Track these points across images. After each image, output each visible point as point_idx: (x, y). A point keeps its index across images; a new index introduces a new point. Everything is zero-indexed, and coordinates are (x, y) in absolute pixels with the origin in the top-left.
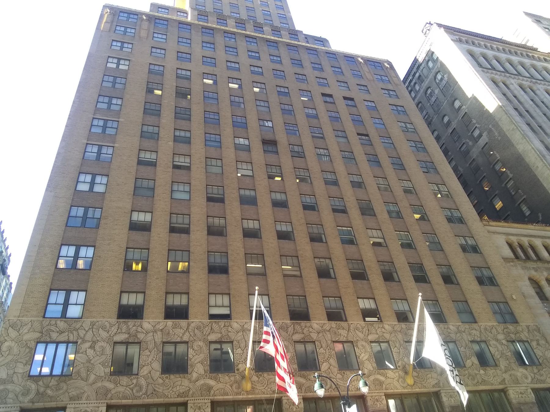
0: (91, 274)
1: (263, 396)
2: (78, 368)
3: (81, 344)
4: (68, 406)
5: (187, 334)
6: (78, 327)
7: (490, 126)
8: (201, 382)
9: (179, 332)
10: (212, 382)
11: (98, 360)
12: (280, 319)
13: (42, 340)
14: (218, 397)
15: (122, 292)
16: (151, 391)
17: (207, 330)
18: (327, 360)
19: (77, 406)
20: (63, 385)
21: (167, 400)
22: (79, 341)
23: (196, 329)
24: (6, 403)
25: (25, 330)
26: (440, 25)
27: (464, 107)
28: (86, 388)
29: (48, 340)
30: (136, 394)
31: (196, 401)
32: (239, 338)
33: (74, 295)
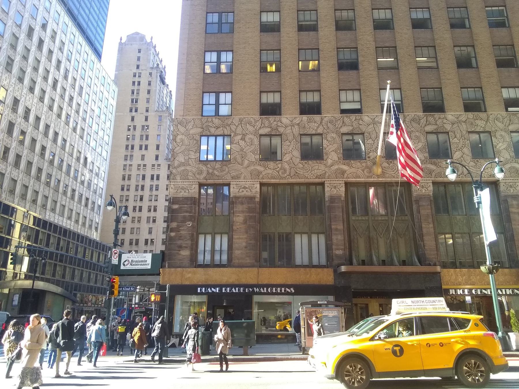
0: (234, 77)
1: (393, 179)
2: (234, 155)
3: (233, 136)
4: (231, 183)
5: (321, 127)
6: (229, 123)
9: (314, 125)
10: (345, 167)
11: (249, 149)
12: (412, 112)
13: (204, 134)
14: (351, 179)
15: (261, 92)
16: (294, 174)
17: (339, 123)
18: (461, 150)
19: (238, 183)
20: (224, 167)
21: (307, 181)
22: (232, 135)
23: (328, 123)
24: (188, 179)
25: (190, 126)
28: (242, 170)
29: (209, 134)
30: (282, 176)
31: (331, 182)
32: (370, 130)
33: (222, 96)
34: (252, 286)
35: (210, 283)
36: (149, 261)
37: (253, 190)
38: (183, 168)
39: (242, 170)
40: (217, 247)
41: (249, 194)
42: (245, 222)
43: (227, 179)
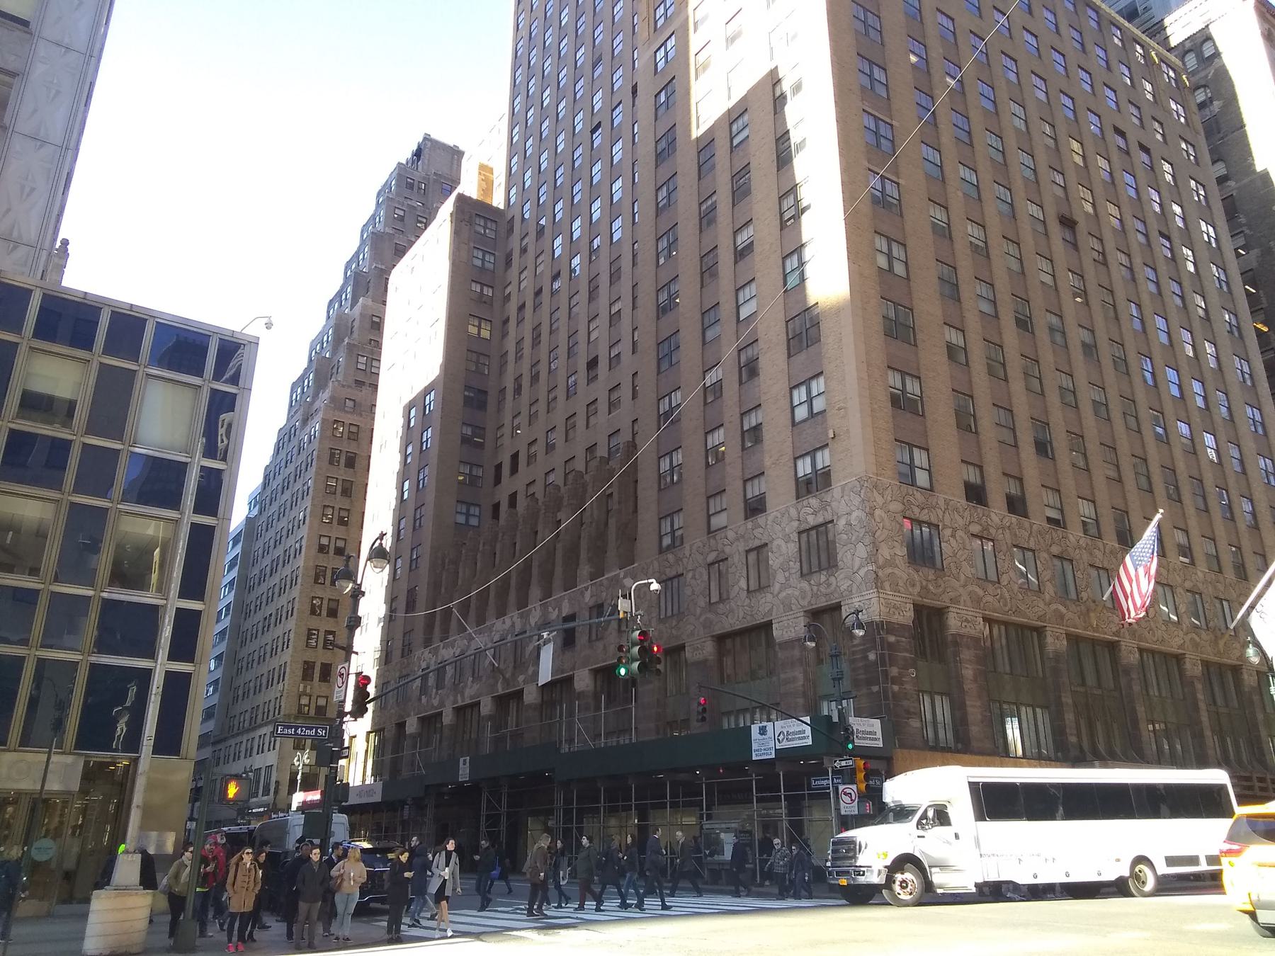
8: (1053, 607)
20: (940, 581)
36: (879, 735)
38: (889, 570)
39: (961, 590)
40: (939, 717)
41: (973, 632)
42: (975, 680)
43: (943, 601)
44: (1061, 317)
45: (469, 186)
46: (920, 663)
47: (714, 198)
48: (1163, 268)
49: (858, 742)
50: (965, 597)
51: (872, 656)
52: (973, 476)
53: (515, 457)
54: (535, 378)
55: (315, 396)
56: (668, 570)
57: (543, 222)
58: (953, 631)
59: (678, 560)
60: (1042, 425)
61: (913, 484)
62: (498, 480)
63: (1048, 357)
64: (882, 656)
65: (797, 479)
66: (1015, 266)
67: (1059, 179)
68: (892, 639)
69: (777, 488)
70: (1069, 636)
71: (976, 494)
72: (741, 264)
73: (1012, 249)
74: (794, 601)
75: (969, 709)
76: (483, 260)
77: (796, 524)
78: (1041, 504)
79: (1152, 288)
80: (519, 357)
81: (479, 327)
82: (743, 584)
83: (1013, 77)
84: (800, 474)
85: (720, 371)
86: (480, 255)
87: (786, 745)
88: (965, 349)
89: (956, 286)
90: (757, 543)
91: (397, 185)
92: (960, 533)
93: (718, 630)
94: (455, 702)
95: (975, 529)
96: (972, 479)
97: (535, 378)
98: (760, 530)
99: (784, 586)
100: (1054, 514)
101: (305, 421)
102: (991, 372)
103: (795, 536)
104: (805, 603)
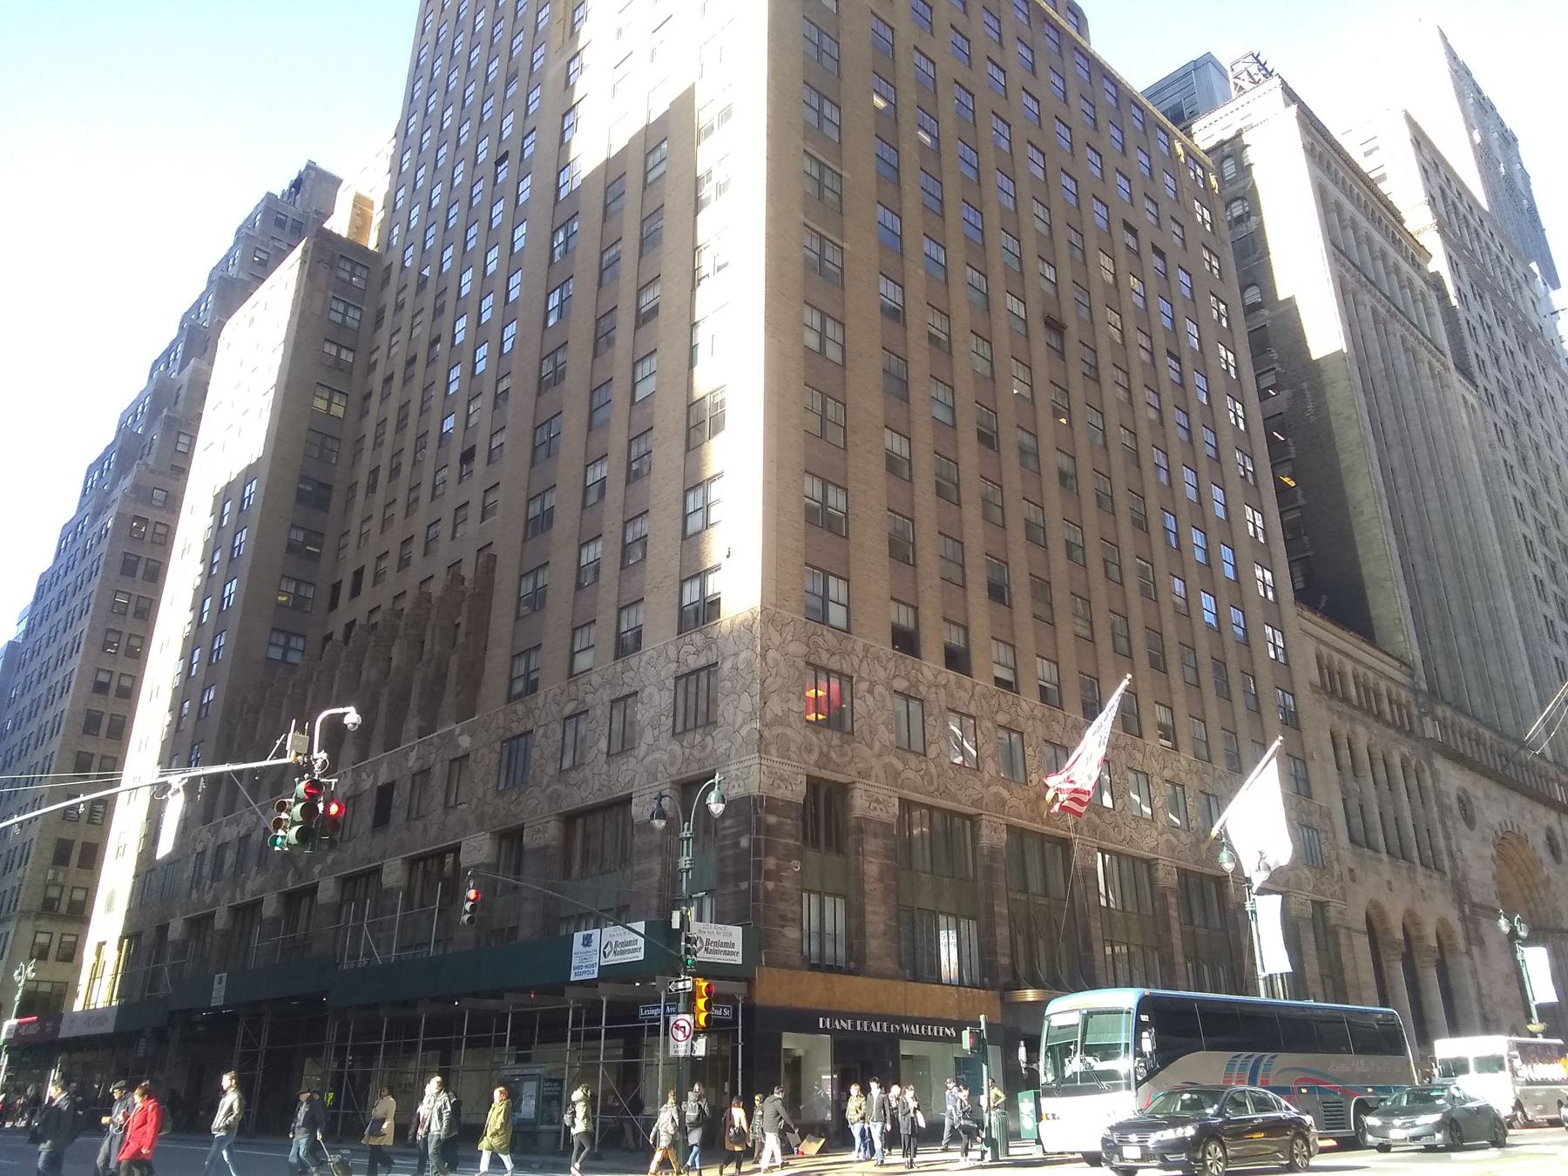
7: (1305, 385)
8: (993, 789)
20: (846, 747)
26: (1290, 96)
27: (1265, 312)
34: (899, 1020)
35: (835, 1007)
36: (739, 948)
37: (891, 811)
38: (778, 730)
39: (873, 761)
40: (829, 927)
41: (884, 816)
42: (881, 880)
44: (1035, 436)
45: (339, 223)
46: (811, 854)
47: (619, 246)
48: (1168, 393)
49: (702, 956)
50: (878, 770)
51: (744, 842)
52: (904, 618)
53: (358, 574)
54: (394, 472)
55: (114, 484)
56: (514, 725)
57: (426, 272)
58: (857, 812)
59: (531, 711)
60: (999, 563)
61: (824, 620)
62: (333, 604)
63: (1014, 481)
64: (756, 843)
65: (681, 609)
66: (982, 366)
67: (1050, 273)
68: (772, 819)
69: (657, 620)
70: (1010, 827)
71: (906, 641)
72: (643, 330)
73: (984, 349)
74: (661, 768)
75: (869, 917)
76: (345, 314)
77: (673, 666)
78: (990, 661)
79: (1153, 415)
80: (378, 443)
81: (330, 402)
82: (603, 745)
83: (1004, 144)
84: (686, 602)
85: (605, 468)
86: (341, 308)
87: (613, 959)
88: (910, 461)
89: (905, 383)
90: (626, 691)
91: (262, 220)
92: (879, 689)
93: (566, 807)
94: (233, 898)
95: (900, 684)
96: (903, 622)
97: (394, 472)
98: (631, 674)
99: (651, 749)
100: (1005, 674)
101: (96, 515)
102: (940, 491)
103: (670, 683)
104: (674, 771)
